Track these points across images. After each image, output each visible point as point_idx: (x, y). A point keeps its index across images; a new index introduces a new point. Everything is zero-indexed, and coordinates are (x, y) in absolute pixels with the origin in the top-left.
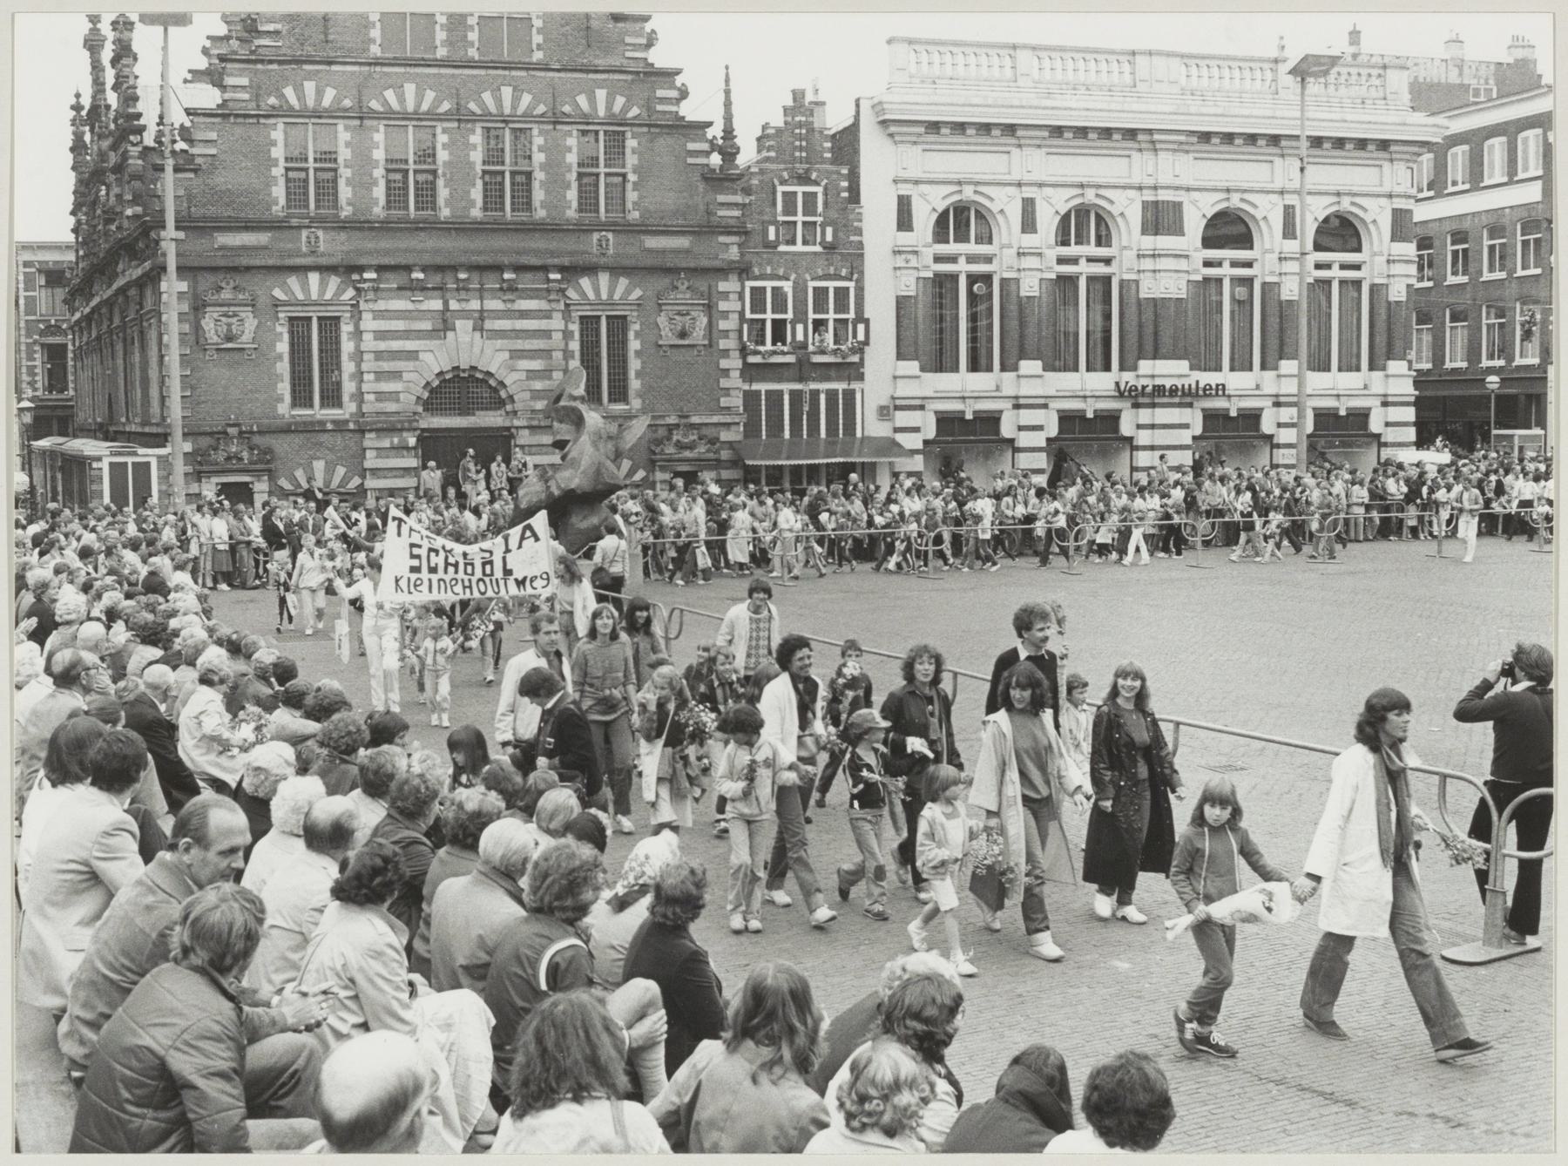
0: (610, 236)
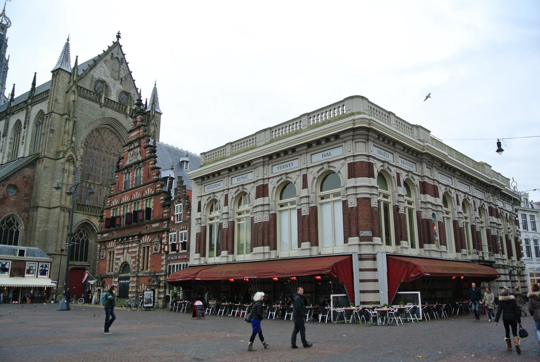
0: (148, 225)
